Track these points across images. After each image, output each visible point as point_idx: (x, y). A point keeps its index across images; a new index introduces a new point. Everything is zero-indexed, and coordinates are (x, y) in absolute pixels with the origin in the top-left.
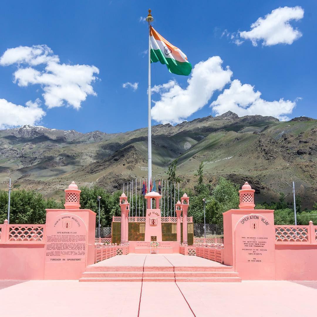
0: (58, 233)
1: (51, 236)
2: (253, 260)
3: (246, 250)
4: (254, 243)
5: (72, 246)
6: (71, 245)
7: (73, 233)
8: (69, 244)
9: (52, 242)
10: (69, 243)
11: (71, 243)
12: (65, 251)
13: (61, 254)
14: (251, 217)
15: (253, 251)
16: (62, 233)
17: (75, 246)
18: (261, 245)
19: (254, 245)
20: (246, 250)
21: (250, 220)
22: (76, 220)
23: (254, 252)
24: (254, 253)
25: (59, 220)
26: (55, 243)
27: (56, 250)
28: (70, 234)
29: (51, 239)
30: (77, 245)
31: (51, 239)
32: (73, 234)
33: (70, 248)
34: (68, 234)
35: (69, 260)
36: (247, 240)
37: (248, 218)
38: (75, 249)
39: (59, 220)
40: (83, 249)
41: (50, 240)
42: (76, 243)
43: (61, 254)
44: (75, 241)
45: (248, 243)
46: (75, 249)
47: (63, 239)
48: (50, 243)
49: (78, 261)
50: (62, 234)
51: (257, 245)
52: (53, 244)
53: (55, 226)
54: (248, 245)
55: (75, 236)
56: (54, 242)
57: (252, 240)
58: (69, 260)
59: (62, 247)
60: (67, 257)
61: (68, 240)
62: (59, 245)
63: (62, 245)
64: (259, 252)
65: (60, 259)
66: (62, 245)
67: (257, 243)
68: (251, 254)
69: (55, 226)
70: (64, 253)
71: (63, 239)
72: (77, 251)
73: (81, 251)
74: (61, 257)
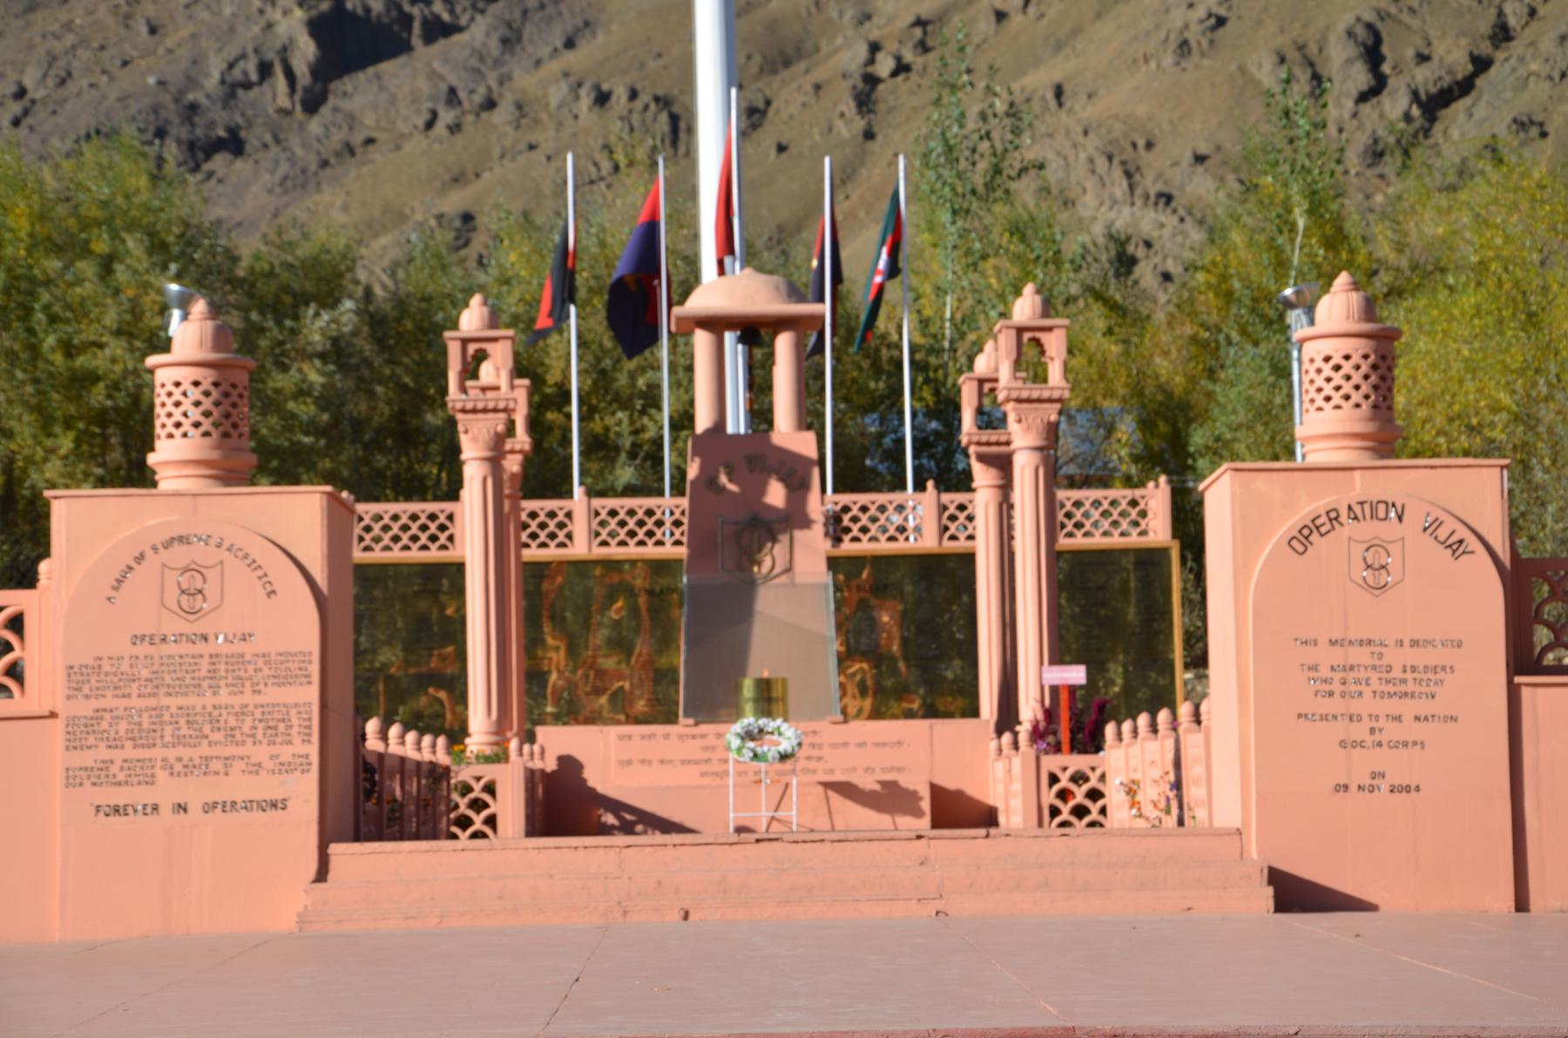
1: (90, 662)
2: (1367, 781)
3: (1324, 718)
4: (1374, 676)
5: (232, 722)
6: (224, 712)
8: (210, 709)
9: (101, 703)
10: (209, 700)
12: (185, 753)
13: (162, 775)
14: (1357, 509)
15: (1366, 724)
17: (248, 722)
18: (1417, 689)
19: (1375, 685)
20: (1324, 718)
21: (1348, 528)
22: (246, 556)
23: (1372, 731)
24: (1377, 737)
25: (140, 558)
26: (124, 702)
27: (129, 752)
30: (258, 715)
33: (218, 736)
34: (201, 647)
35: (209, 808)
36: (1327, 657)
37: (1333, 515)
38: (249, 741)
39: (140, 558)
40: (297, 740)
41: (86, 689)
42: (248, 698)
43: (162, 775)
44: (248, 689)
45: (1337, 676)
48: (85, 708)
51: (1390, 688)
52: (107, 716)
54: (1336, 687)
56: (109, 702)
57: (1360, 656)
58: (209, 808)
59: (168, 730)
60: (196, 791)
64: (1409, 730)
65: (155, 808)
67: (1397, 673)
68: (1355, 744)
70: (178, 767)
71: (168, 680)
72: (260, 753)
73: (286, 753)
74: (166, 790)
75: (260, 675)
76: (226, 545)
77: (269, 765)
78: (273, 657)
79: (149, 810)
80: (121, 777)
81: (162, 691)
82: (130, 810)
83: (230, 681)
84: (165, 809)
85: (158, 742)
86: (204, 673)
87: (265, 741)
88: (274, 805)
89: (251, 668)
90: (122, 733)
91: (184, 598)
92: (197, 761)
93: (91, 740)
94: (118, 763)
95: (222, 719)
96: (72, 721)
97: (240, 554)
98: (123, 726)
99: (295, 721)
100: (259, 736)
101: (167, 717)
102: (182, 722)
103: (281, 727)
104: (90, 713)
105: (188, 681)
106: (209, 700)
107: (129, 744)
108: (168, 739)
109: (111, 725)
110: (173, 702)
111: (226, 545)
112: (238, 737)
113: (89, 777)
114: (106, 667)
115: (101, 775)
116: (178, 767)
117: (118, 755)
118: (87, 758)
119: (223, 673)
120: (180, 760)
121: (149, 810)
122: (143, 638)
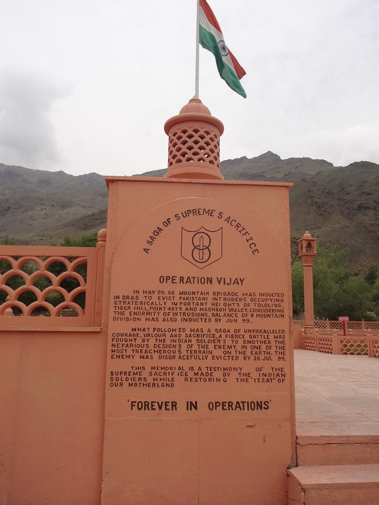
0: (162, 279)
1: (131, 294)
5: (229, 342)
7: (227, 281)
8: (213, 332)
9: (137, 324)
10: (213, 326)
11: (219, 326)
12: (196, 364)
13: (179, 380)
16: (182, 279)
22: (238, 226)
25: (168, 222)
26: (152, 325)
27: (156, 361)
28: (215, 287)
29: (132, 310)
30: (247, 338)
31: (132, 307)
32: (222, 288)
33: (219, 352)
34: (206, 287)
38: (241, 356)
39: (168, 222)
40: (274, 357)
42: (241, 325)
43: (179, 380)
44: (240, 318)
46: (241, 356)
47: (184, 308)
49: (258, 413)
50: (179, 287)
52: (141, 334)
53: (146, 250)
55: (240, 296)
56: (142, 324)
58: (213, 406)
59: (184, 346)
60: (205, 393)
61: (210, 314)
62: (168, 334)
63: (183, 334)
65: (174, 405)
66: (183, 334)
69: (146, 250)
70: (191, 374)
71: (184, 308)
72: (249, 366)
74: (181, 393)
75: (248, 309)
76: (225, 217)
77: (255, 375)
78: (257, 296)
79: (170, 407)
80: (150, 380)
81: (179, 318)
82: (156, 406)
83: (228, 312)
84: (181, 406)
85: (177, 355)
86: (209, 305)
87: (252, 357)
88: (259, 405)
89: (241, 304)
90: (151, 347)
91: (196, 251)
92: (204, 371)
93: (129, 351)
94: (148, 369)
95: (222, 340)
96: (118, 336)
97: (234, 224)
98: (152, 341)
99: (273, 344)
100: (248, 353)
101: (183, 337)
102: (194, 340)
103: (263, 347)
104: (129, 331)
105: (198, 311)
106: (213, 326)
107: (156, 356)
108: (184, 353)
109: (143, 341)
110: (188, 326)
111: (225, 217)
112: (233, 354)
113: (127, 379)
114: (142, 298)
115: (135, 378)
116: (191, 374)
117: (148, 364)
118: (124, 365)
119: (222, 306)
120: (192, 369)
121: (170, 407)
122: (168, 278)
